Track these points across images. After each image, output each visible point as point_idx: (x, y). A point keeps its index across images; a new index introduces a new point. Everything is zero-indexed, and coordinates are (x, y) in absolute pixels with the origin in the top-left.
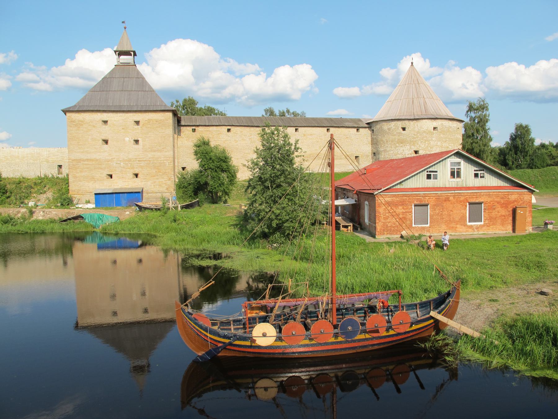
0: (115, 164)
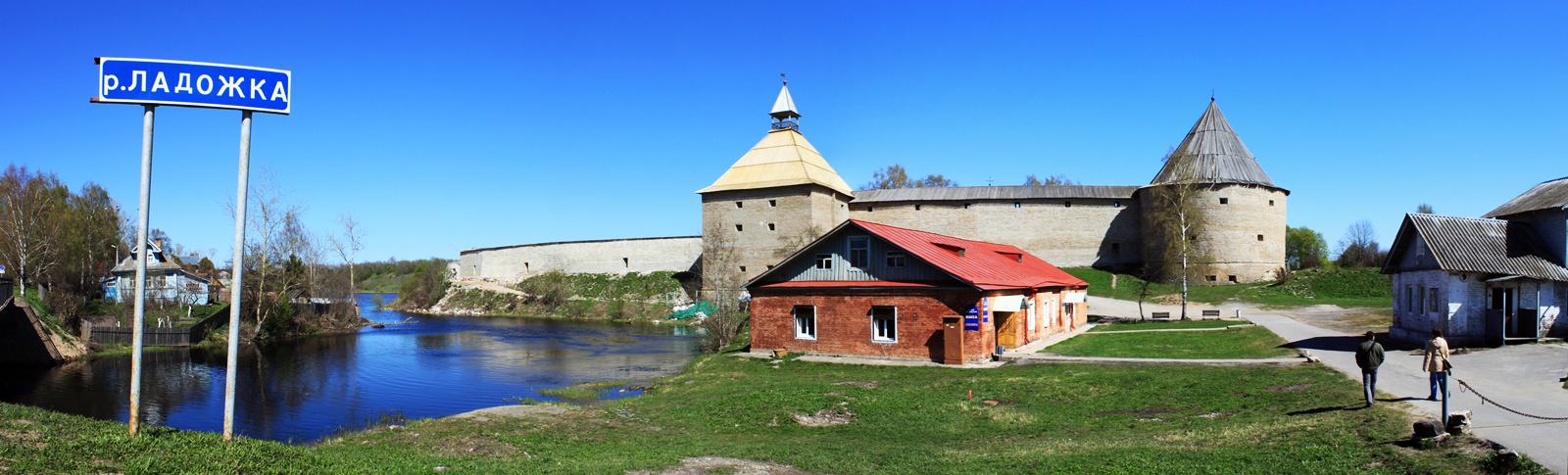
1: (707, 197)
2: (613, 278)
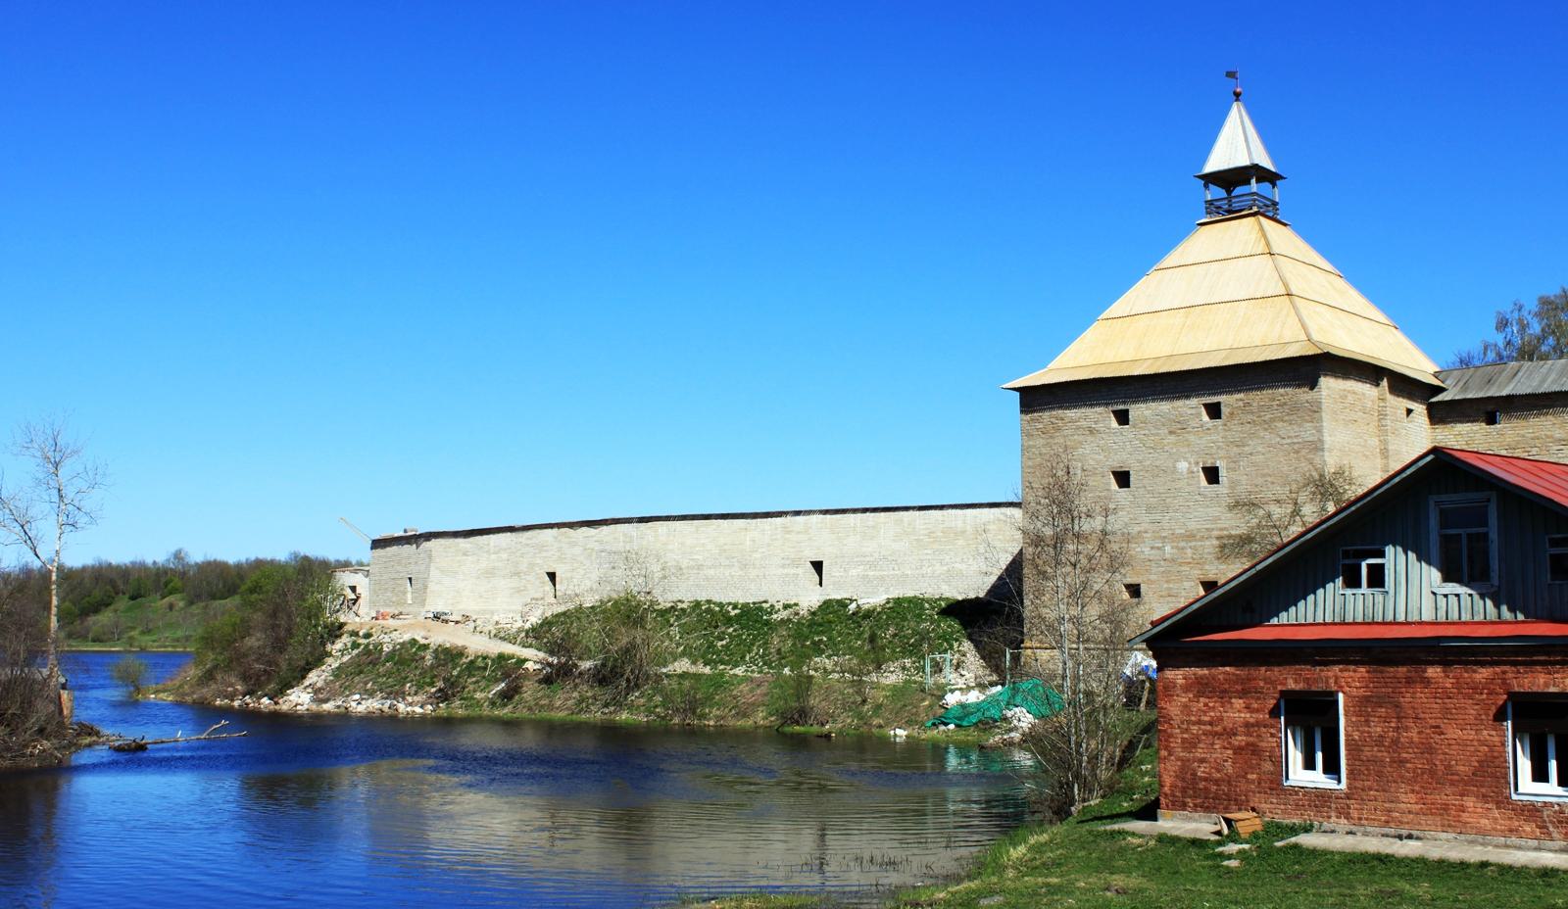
0: (1147, 550)
1: (1034, 399)
2: (784, 614)
